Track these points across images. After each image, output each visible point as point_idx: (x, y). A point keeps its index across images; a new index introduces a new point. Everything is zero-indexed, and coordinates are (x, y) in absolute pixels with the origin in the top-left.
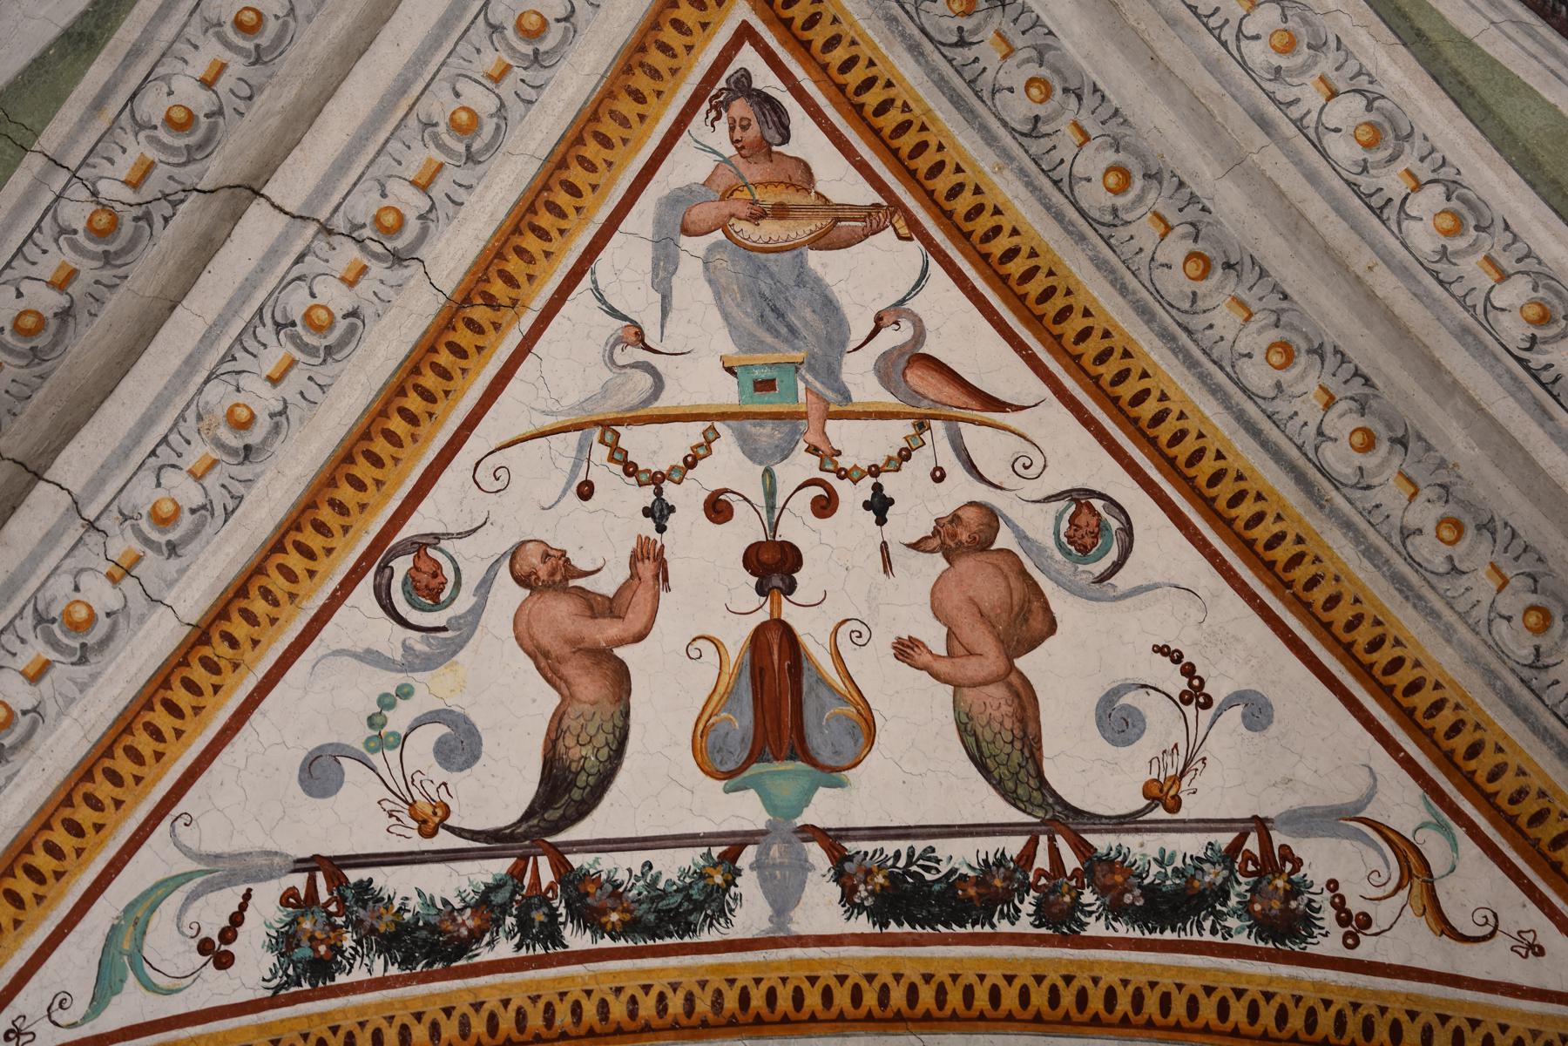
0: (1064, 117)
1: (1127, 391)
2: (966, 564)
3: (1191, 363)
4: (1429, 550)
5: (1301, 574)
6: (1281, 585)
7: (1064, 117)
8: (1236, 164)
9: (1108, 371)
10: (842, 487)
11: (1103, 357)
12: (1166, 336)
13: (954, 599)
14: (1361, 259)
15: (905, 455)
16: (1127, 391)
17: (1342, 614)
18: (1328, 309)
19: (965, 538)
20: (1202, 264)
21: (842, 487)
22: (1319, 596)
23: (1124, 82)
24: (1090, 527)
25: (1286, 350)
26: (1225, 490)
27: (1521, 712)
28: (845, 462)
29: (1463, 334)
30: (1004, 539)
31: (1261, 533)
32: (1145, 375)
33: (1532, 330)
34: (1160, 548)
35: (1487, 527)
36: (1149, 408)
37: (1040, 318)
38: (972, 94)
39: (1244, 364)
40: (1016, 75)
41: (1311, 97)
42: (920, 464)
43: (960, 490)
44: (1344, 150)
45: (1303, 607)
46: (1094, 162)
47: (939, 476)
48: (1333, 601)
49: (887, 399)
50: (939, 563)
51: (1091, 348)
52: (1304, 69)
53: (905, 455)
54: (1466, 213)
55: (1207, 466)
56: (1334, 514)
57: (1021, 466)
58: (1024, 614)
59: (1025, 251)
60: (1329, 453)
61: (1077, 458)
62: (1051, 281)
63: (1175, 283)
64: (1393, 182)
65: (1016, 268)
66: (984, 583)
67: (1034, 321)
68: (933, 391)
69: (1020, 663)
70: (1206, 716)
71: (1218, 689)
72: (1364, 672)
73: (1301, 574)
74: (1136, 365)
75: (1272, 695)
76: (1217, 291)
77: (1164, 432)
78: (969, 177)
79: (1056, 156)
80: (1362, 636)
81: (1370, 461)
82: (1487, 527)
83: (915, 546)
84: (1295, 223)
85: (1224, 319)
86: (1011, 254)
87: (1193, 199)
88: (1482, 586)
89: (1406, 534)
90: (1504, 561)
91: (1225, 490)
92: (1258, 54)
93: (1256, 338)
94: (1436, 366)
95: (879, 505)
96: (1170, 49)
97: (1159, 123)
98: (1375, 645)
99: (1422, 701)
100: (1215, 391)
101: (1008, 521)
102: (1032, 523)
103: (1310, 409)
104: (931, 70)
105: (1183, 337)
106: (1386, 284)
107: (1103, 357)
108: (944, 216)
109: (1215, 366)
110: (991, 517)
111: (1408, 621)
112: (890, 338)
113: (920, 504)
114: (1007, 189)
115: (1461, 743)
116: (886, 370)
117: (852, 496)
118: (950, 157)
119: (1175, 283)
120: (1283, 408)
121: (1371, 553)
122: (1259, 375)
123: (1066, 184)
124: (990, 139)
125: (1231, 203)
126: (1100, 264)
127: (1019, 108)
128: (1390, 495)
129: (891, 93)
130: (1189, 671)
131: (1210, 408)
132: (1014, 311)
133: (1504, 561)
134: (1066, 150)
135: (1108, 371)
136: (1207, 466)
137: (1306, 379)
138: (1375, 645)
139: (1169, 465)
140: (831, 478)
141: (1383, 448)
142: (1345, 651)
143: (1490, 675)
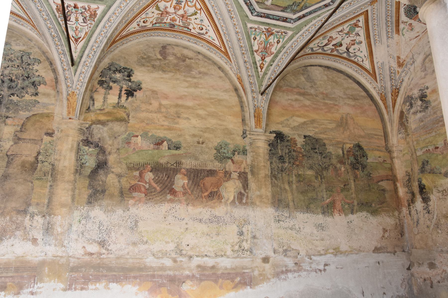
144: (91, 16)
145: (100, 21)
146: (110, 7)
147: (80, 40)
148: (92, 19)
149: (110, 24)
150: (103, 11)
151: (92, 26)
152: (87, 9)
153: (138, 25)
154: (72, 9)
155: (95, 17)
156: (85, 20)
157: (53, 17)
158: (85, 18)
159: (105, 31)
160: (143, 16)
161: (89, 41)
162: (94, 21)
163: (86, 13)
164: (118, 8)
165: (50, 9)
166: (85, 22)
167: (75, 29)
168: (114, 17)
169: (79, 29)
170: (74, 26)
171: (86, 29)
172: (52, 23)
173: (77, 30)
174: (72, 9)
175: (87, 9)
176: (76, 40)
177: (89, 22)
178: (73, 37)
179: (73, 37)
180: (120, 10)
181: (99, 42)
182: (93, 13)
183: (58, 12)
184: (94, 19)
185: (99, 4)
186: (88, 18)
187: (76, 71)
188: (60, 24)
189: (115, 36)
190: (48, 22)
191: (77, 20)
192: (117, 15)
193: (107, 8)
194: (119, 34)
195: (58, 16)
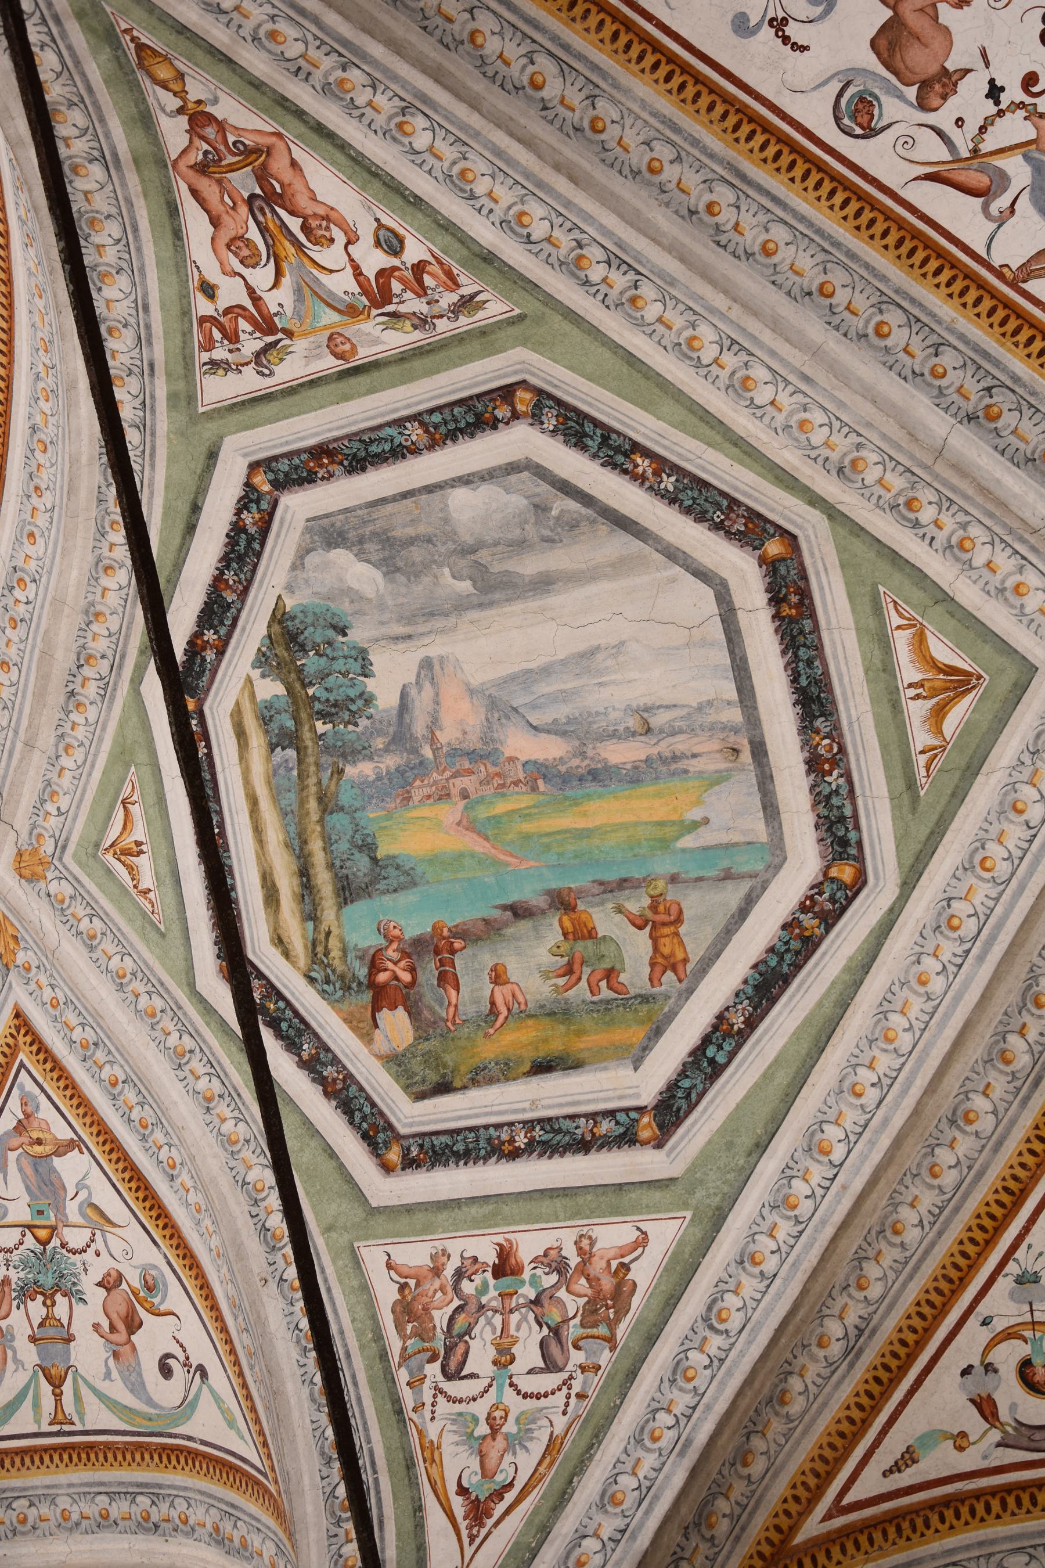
0: (921, 359)
1: (854, 206)
2: (933, 69)
3: (819, 232)
4: (665, 153)
5: (732, 120)
6: (743, 110)
7: (921, 359)
8: (816, 352)
9: (867, 215)
10: (1020, 96)
11: (872, 223)
12: (837, 245)
13: (938, 44)
14: (736, 312)
15: (983, 129)
16: (854, 206)
17: (704, 101)
18: (747, 279)
19: (935, 87)
20: (825, 291)
21: (1020, 96)
22: (720, 109)
23: (890, 386)
24: (860, 115)
25: (767, 252)
26: (785, 160)
27: (595, 67)
28: (1022, 113)
29: (672, 282)
30: (911, 92)
31: (759, 139)
32: (845, 218)
33: (639, 292)
34: (815, 113)
35: (636, 173)
36: (838, 199)
37: (913, 238)
38: (978, 361)
39: (789, 238)
40: (954, 377)
41: (783, 399)
42: (972, 126)
43: (943, 118)
44: (759, 373)
45: (728, 100)
46: (898, 337)
47: (959, 122)
48: (711, 108)
49: (1000, 162)
50: (950, 65)
51: (879, 227)
52: (791, 414)
53: (983, 129)
54: (687, 350)
55: (798, 172)
56: (721, 161)
57: (910, 142)
58: (892, 47)
59: (930, 276)
60: (730, 196)
61: (876, 157)
62: (910, 262)
63: (838, 277)
64: (730, 360)
65: (933, 265)
66: (920, 60)
67: (917, 235)
68: (972, 176)
69: (889, 13)
70: (771, 14)
71: (767, 33)
72: (686, 69)
73: (732, 120)
74: (852, 223)
75: (735, 39)
76: (813, 278)
77: (827, 186)
78: (971, 312)
79: (921, 336)
80: (690, 91)
81: (707, 197)
82: (636, 173)
83: (968, 71)
84: (776, 325)
85: (805, 262)
86: (937, 272)
87: (837, 328)
88: (631, 139)
89: (678, 159)
90: (623, 156)
91: (785, 160)
92: (817, 417)
93: (785, 255)
94: (682, 260)
95: (994, 91)
96: (867, 410)
97: (864, 366)
98: (682, 87)
99: (650, 59)
100: (802, 219)
101: (911, 105)
102: (896, 109)
103: (747, 220)
104: (1005, 369)
105: (827, 246)
106: (720, 301)
107: (872, 223)
108: (982, 285)
109: (807, 234)
110: (923, 105)
111: (666, 106)
112: (1003, 202)
113: (969, 100)
114: (945, 310)
115: (623, 39)
116: (1003, 179)
117: (1014, 93)
118: (985, 321)
119: (838, 277)
120: (762, 218)
121: (695, 142)
122: (779, 234)
123: (912, 321)
124: (962, 337)
125: (815, 330)
126: (884, 278)
127: (948, 359)
128: (692, 180)
129: (1026, 351)
130: (786, 39)
131: (804, 207)
132: (929, 238)
133: (623, 156)
134: (916, 340)
135: (867, 215)
136: (798, 172)
137: (752, 238)
138: (682, 87)
139: (821, 167)
140: (1028, 100)
141: (701, 207)
142: (698, 79)
143: (616, 86)
144: (591, 1314)
145: (651, 1338)
146: (718, 1218)
147: (500, 1509)
148: (602, 1330)
149: (716, 1342)
150: (675, 1257)
151: (596, 1381)
152: (574, 1260)
153: (986, 1407)
154: (484, 1289)
155: (622, 1311)
156: (554, 1349)
157: (369, 1368)
158: (556, 1331)
159: (682, 1401)
160: (1002, 1305)
161: (562, 1499)
162: (611, 1341)
163: (562, 1294)
164: (774, 1217)
165: (361, 1313)
166: (551, 1366)
167: (483, 1429)
168: (750, 1286)
169: (510, 1427)
170: (480, 1409)
171: (556, 1418)
173: (494, 1431)
174: (484, 1289)
175: (574, 1260)
176: (478, 1512)
178: (462, 1491)
179: (462, 1491)
180: (785, 1229)
181: (631, 1498)
182: (607, 1284)
183: (399, 1327)
184: (612, 1325)
185: (649, 1209)
186: (573, 1330)
188: (399, 1412)
189: (780, 1488)
191: (504, 1358)
192: (770, 1264)
193: (698, 1233)
194: (825, 1479)
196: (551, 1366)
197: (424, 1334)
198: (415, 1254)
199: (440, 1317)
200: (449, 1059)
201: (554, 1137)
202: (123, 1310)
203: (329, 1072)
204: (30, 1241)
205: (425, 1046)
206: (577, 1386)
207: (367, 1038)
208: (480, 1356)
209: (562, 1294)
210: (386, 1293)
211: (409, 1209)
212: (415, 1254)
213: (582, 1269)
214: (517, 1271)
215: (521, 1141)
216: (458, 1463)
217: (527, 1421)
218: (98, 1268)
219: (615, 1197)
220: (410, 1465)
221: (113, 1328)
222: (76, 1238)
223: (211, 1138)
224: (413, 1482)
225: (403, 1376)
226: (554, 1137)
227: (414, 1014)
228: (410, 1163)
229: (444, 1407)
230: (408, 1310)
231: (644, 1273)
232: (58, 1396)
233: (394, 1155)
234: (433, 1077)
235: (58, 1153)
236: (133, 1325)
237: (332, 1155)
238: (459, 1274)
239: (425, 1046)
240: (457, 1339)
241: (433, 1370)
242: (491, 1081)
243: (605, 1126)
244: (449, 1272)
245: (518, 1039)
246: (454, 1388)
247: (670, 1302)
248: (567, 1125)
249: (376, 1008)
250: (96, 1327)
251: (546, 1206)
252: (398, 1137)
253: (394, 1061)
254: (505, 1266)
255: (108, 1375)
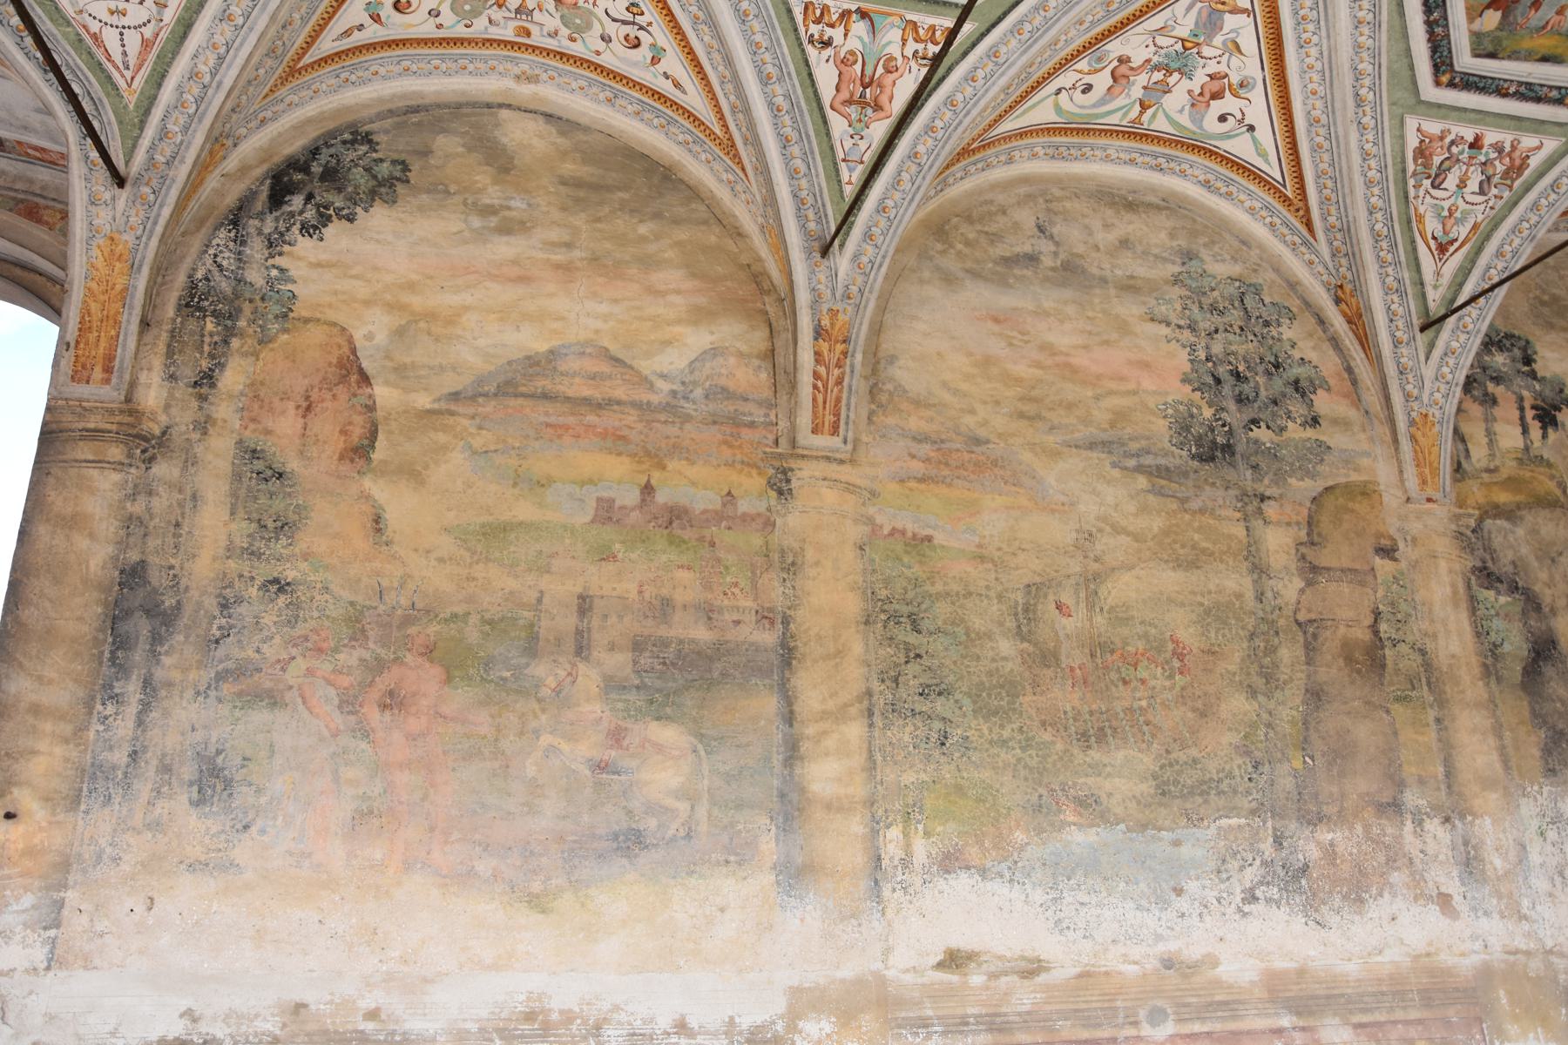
145: (1527, 188)
147: (1452, 249)
149: (1553, 197)
150: (1550, 157)
151: (1500, 203)
152: (1508, 149)
154: (1462, 153)
155: (1519, 175)
156: (1485, 186)
157: (1395, 174)
158: (1489, 178)
159: (1534, 219)
161: (1479, 250)
162: (1510, 187)
163: (1497, 163)
165: (1397, 148)
166: (1482, 192)
167: (1446, 213)
169: (1458, 215)
170: (1446, 204)
171: (1479, 215)
172: (1384, 195)
173: (1451, 215)
174: (1462, 153)
175: (1508, 149)
177: (1494, 191)
178: (1434, 238)
179: (1434, 238)
181: (1509, 256)
182: (1518, 162)
183: (1415, 160)
186: (1496, 180)
187: (1431, 346)
188: (1407, 197)
190: (1376, 191)
191: (1462, 184)
195: (1409, 173)
196: (1482, 192)
197: (1426, 166)
198: (1433, 127)
199: (1437, 160)
200: (1505, 43)
201: (1529, 92)
202: (1215, 89)
203: (1439, 30)
204: (1179, 47)
205: (1499, 33)
206: (1491, 204)
207: (1471, 19)
208: (1451, 181)
209: (1497, 163)
210: (1412, 142)
211: (1440, 106)
212: (1433, 127)
213: (1509, 155)
214: (1480, 148)
215: (1512, 90)
216: (1432, 225)
217: (1465, 214)
218: (1212, 68)
219: (1538, 126)
220: (1409, 222)
221: (1201, 94)
222: (1206, 51)
223: (1350, 42)
224: (1410, 229)
225: (1411, 182)
226: (1529, 92)
227: (1504, 17)
228: (1451, 85)
229: (1428, 199)
230: (1421, 152)
231: (1534, 162)
232: (1141, 113)
233: (1445, 79)
234: (1490, 48)
235: (1230, 12)
236: (1217, 96)
237: (1412, 67)
238: (1453, 143)
239: (1499, 33)
240: (1442, 171)
241: (1427, 183)
242: (1517, 59)
243: (1554, 94)
244: (1448, 140)
245: (1544, 43)
246: (1435, 192)
247: (1541, 174)
248: (1537, 88)
249: (1488, 7)
250: (1190, 92)
251: (1508, 122)
252: (1452, 70)
253: (1477, 37)
254: (1476, 144)
255: (1181, 111)
